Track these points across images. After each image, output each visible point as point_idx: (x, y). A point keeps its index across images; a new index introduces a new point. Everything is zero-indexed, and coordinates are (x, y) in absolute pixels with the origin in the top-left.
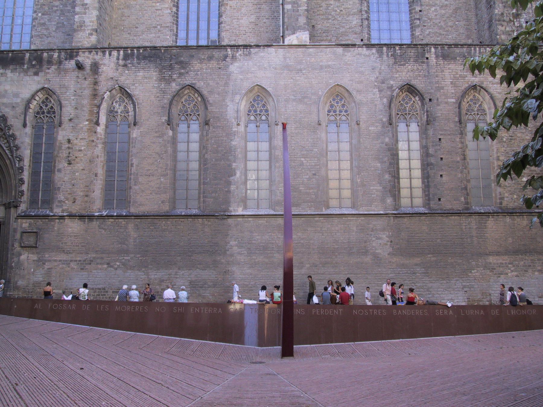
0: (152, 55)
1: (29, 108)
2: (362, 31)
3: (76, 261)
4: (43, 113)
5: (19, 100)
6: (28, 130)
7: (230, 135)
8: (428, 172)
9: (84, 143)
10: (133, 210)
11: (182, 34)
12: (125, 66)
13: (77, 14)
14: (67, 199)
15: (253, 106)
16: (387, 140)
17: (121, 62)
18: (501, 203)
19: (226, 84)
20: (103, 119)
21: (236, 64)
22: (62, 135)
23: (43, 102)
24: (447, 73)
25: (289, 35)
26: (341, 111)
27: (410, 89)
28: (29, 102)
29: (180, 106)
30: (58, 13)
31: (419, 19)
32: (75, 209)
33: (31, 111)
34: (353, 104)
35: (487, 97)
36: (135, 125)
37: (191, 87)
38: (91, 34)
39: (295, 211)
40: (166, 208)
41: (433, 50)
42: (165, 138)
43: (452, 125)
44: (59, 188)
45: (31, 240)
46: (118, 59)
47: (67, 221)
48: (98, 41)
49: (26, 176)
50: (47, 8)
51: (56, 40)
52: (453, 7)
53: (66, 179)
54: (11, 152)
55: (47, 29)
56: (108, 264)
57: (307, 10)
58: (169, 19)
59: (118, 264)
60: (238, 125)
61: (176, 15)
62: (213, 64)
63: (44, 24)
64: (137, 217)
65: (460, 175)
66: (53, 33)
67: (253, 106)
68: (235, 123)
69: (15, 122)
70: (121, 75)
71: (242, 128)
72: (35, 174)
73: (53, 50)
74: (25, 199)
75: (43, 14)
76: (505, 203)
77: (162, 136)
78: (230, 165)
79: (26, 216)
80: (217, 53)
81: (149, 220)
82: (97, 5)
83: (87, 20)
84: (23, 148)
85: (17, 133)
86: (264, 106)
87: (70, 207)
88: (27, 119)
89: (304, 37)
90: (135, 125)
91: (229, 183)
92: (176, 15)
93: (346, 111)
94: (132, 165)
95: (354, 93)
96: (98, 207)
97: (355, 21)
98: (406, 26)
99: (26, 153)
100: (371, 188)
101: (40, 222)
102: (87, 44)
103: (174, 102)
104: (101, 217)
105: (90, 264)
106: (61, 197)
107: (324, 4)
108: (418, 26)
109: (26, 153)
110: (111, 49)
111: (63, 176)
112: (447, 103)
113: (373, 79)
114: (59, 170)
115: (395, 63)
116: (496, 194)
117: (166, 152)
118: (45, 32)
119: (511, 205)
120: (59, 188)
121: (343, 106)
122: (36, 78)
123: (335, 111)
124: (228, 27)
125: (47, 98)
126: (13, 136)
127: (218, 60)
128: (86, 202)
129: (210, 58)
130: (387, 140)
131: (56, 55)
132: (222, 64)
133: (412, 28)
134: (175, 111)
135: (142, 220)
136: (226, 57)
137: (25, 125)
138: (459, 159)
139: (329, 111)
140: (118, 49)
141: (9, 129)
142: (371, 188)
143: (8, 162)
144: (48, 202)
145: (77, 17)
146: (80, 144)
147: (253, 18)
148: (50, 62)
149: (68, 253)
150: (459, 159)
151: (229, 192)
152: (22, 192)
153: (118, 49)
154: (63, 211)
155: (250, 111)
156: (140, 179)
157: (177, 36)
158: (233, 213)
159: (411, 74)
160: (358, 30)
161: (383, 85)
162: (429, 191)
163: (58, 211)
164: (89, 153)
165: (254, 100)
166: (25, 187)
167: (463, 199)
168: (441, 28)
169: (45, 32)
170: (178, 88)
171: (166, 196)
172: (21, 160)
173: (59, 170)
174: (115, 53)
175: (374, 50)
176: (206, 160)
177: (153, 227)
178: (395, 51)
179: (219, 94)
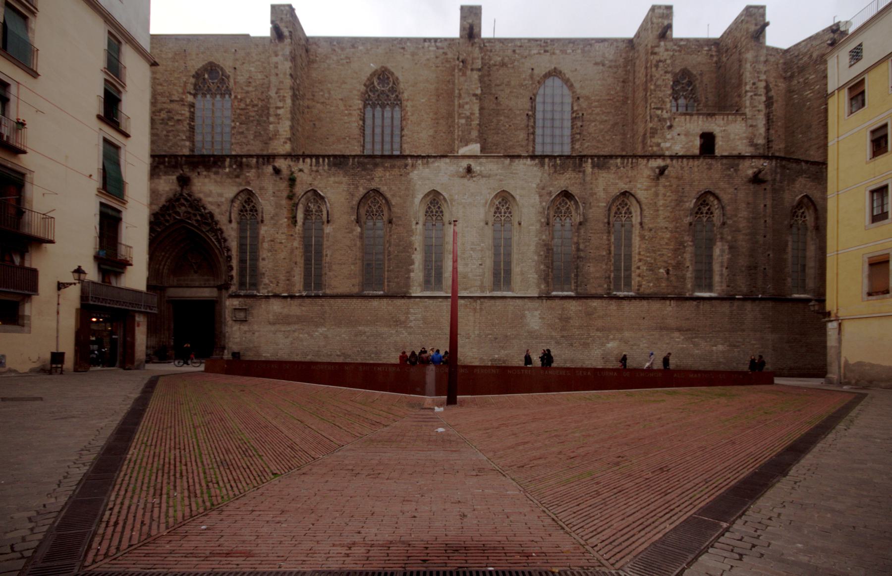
0: (339, 161)
2: (527, 145)
4: (246, 211)
5: (223, 200)
6: (234, 225)
7: (411, 232)
9: (284, 237)
10: (328, 292)
11: (368, 146)
12: (317, 171)
13: (271, 123)
14: (271, 282)
15: (429, 208)
16: (544, 237)
17: (314, 168)
19: (407, 189)
20: (300, 216)
21: (415, 172)
22: (263, 230)
23: (246, 202)
24: (600, 180)
25: (462, 147)
26: (505, 213)
27: (566, 195)
28: (233, 201)
29: (366, 207)
30: (255, 123)
31: (580, 134)
32: (281, 290)
35: (634, 202)
36: (328, 222)
37: (376, 191)
38: (285, 143)
39: (462, 293)
40: (356, 290)
41: (590, 160)
42: (354, 233)
43: (601, 225)
44: (264, 274)
45: (241, 315)
46: (311, 165)
47: (272, 300)
48: (293, 149)
49: (235, 263)
50: (243, 118)
51: (256, 148)
52: (611, 123)
53: (269, 266)
54: (220, 243)
55: (246, 137)
57: (479, 125)
58: (356, 132)
60: (417, 223)
61: (363, 129)
62: (396, 171)
63: (242, 133)
65: (604, 267)
66: (252, 142)
67: (429, 208)
68: (414, 222)
69: (221, 218)
70: (314, 179)
71: (420, 226)
72: (242, 261)
73: (251, 156)
75: (241, 124)
76: (642, 290)
77: (351, 231)
78: (410, 257)
79: (237, 296)
80: (398, 163)
82: (289, 116)
83: (281, 130)
84: (230, 240)
85: (224, 228)
86: (439, 208)
87: (273, 288)
89: (474, 148)
90: (328, 222)
91: (409, 271)
92: (363, 129)
93: (510, 213)
94: (326, 255)
95: (518, 198)
97: (522, 135)
98: (567, 140)
99: (234, 245)
101: (249, 301)
102: (282, 152)
103: (362, 204)
104: (301, 297)
106: (266, 280)
107: (494, 120)
108: (579, 140)
109: (234, 245)
110: (304, 156)
111: (266, 265)
113: (534, 186)
114: (263, 259)
117: (355, 245)
118: (244, 140)
119: (648, 291)
120: (264, 274)
121: (508, 208)
122: (237, 180)
123: (500, 213)
124: (409, 140)
125: (249, 199)
126: (220, 229)
127: (399, 168)
128: (288, 285)
129: (393, 167)
130: (544, 237)
131: (254, 160)
132: (403, 171)
133: (572, 142)
134: (363, 211)
136: (406, 165)
138: (604, 253)
139: (495, 213)
140: (311, 157)
141: (216, 224)
143: (217, 251)
144: (255, 285)
145: (271, 126)
146: (281, 237)
147: (431, 132)
148: (249, 166)
150: (604, 253)
151: (409, 278)
152: (232, 277)
153: (311, 157)
154: (268, 292)
155: (427, 212)
156: (334, 267)
157: (364, 146)
158: (413, 295)
159: (568, 181)
160: (524, 143)
163: (263, 292)
164: (289, 245)
165: (431, 203)
167: (605, 286)
168: (599, 141)
169: (244, 140)
170: (365, 191)
172: (229, 250)
173: (263, 259)
174: (308, 160)
176: (389, 252)
178: (555, 162)
179: (400, 197)
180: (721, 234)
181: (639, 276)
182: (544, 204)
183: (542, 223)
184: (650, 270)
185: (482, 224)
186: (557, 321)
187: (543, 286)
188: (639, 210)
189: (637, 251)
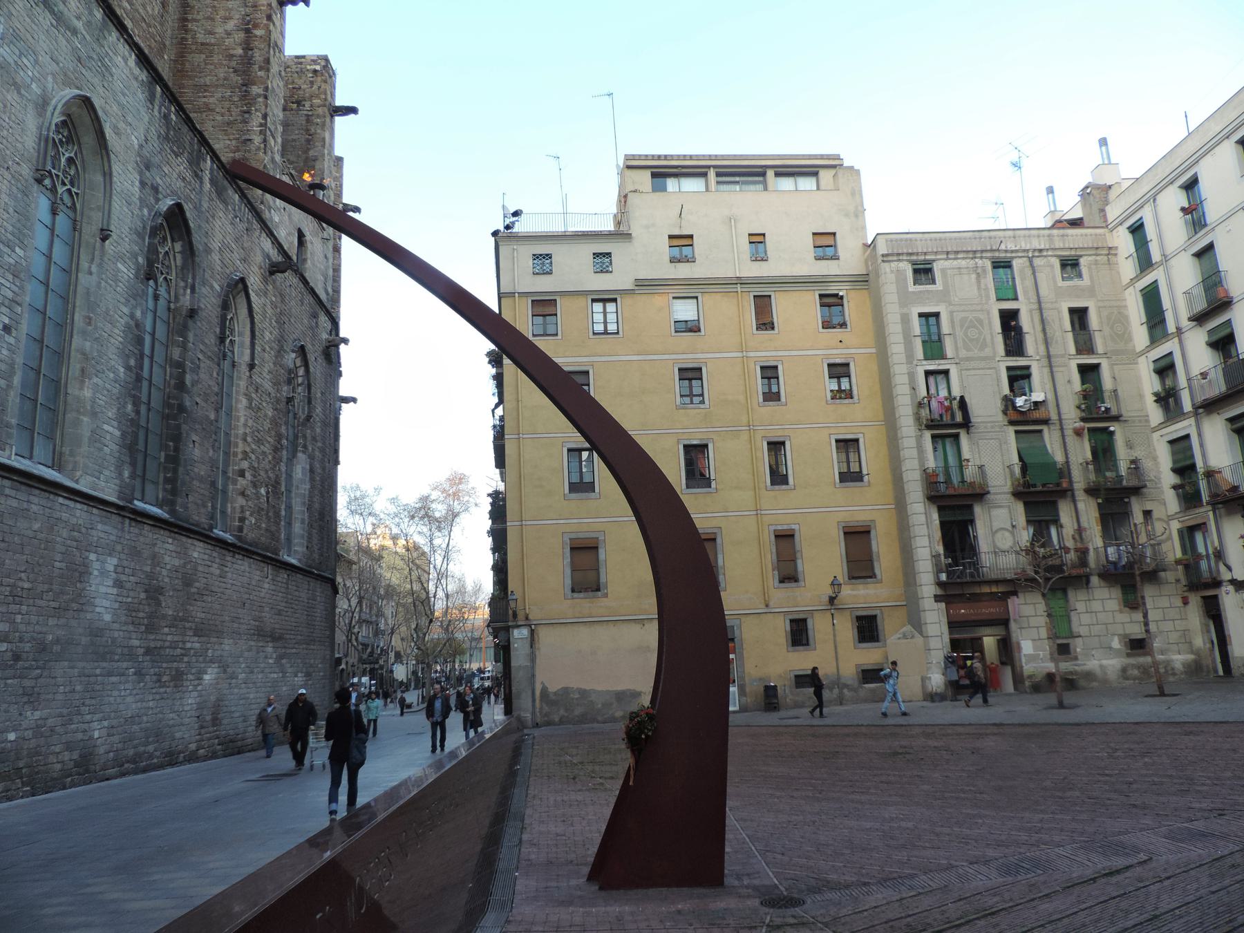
8: (178, 427)
18: (240, 529)
34: (100, 178)
35: (243, 312)
76: (245, 531)
100: (106, 427)
112: (212, 287)
115: (167, 138)
116: (234, 509)
142: (106, 427)
161: (147, 174)
162: (175, 471)
175: (144, 76)
180: (305, 437)
181: (243, 494)
182: (145, 211)
183: (138, 270)
184: (255, 485)
185: (26, 171)
186: (143, 596)
187: (126, 474)
188: (248, 333)
189: (241, 431)
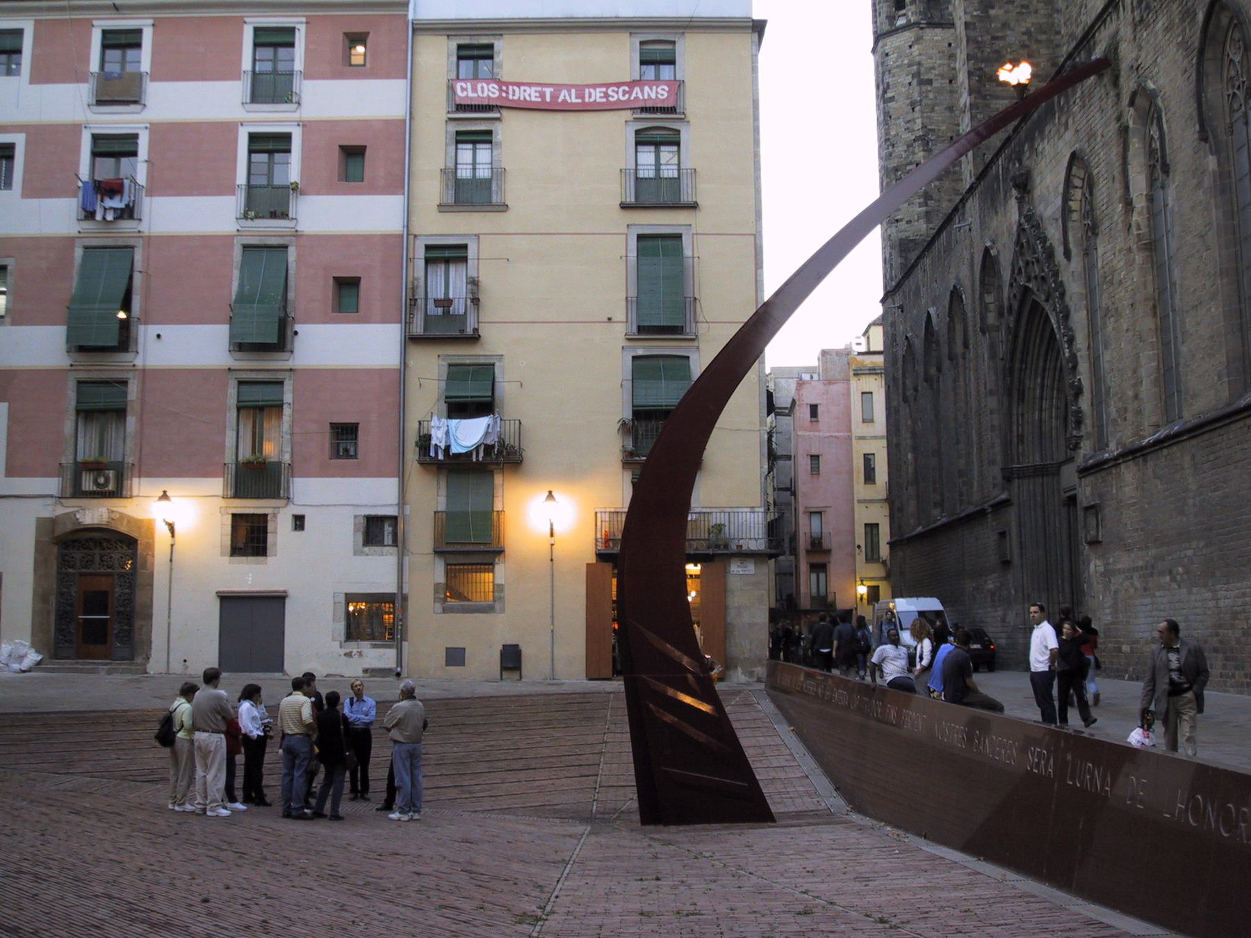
1: (1072, 211)
3: (1135, 569)
33: (1075, 216)
56: (1170, 573)
59: (1180, 569)
64: (1194, 431)
74: (1090, 429)
81: (1206, 437)
88: (1071, 239)
96: (1154, 419)
105: (1152, 575)
135: (1199, 439)
137: (1067, 254)
149: (1128, 549)
163: (1113, 449)
166: (1085, 403)
171: (1222, 358)
177: (1212, 457)
